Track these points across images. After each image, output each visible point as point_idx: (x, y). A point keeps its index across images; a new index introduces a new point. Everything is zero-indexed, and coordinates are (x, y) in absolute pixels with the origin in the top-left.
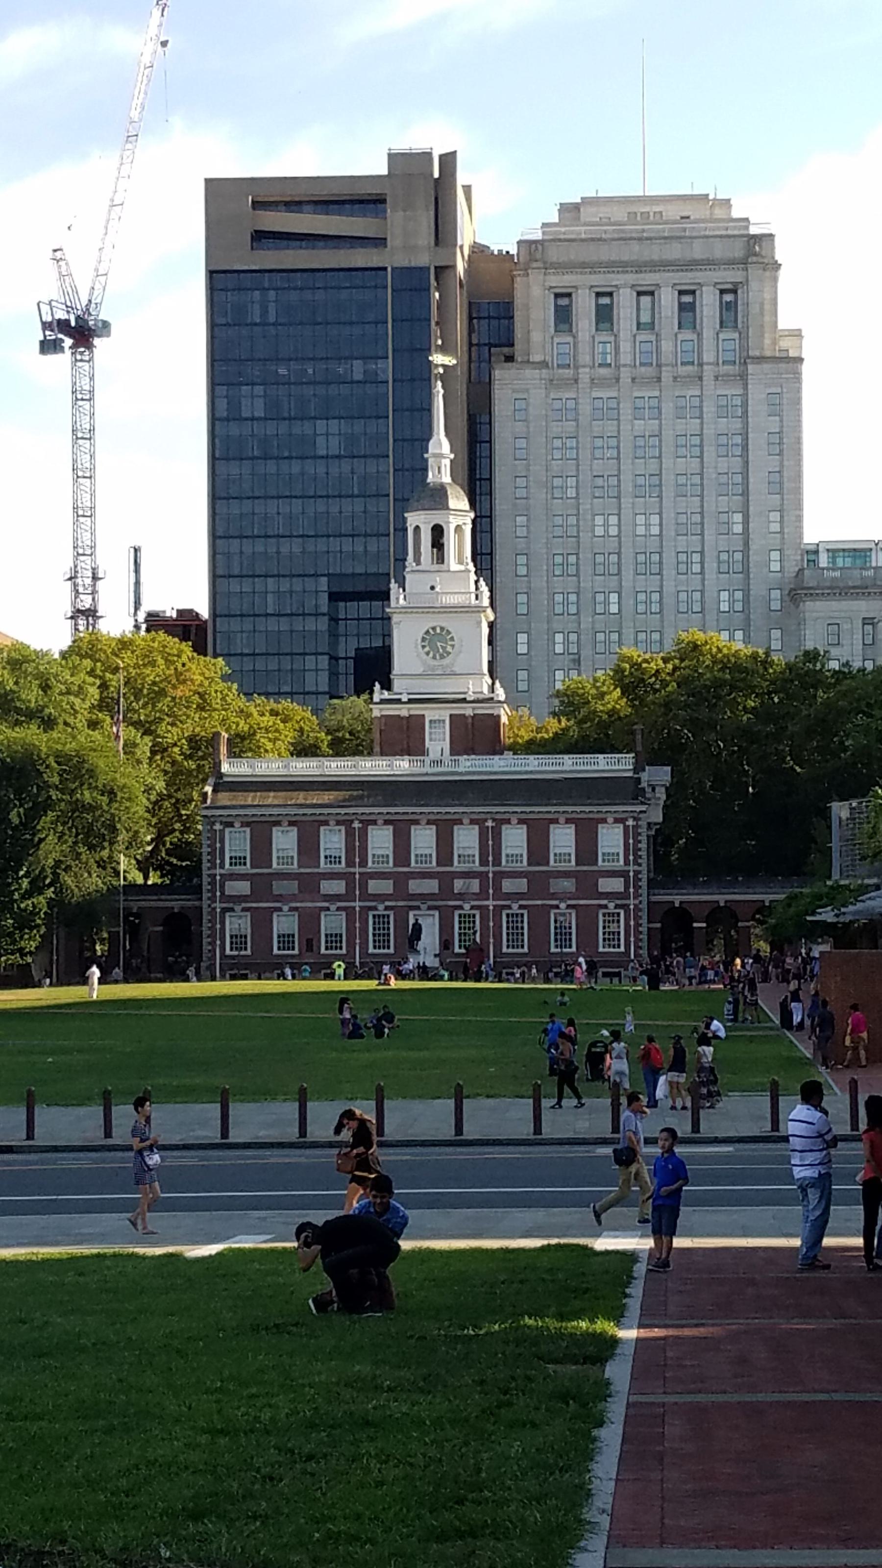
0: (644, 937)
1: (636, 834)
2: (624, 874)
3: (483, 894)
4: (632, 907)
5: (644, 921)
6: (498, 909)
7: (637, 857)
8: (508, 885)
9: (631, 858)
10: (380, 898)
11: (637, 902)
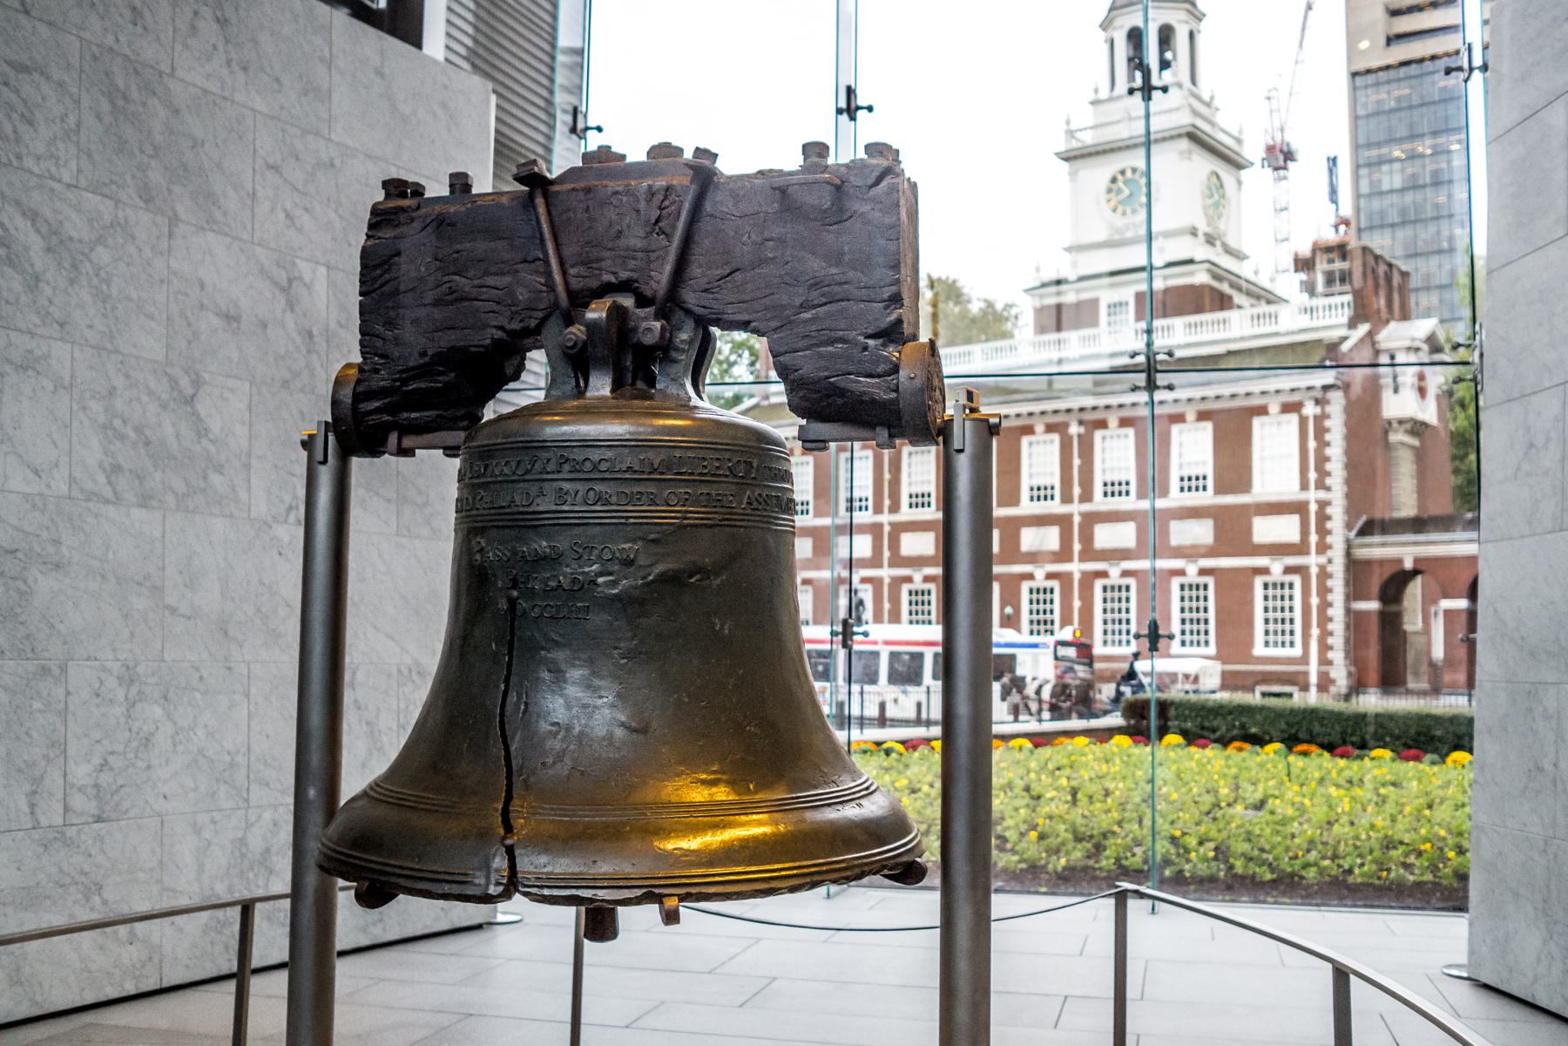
0: (1338, 626)
1: (1321, 431)
2: (1299, 508)
3: (1064, 554)
4: (1314, 571)
5: (1337, 596)
6: (1089, 578)
7: (1323, 473)
8: (1106, 536)
9: (1313, 476)
10: (917, 562)
11: (1322, 560)
